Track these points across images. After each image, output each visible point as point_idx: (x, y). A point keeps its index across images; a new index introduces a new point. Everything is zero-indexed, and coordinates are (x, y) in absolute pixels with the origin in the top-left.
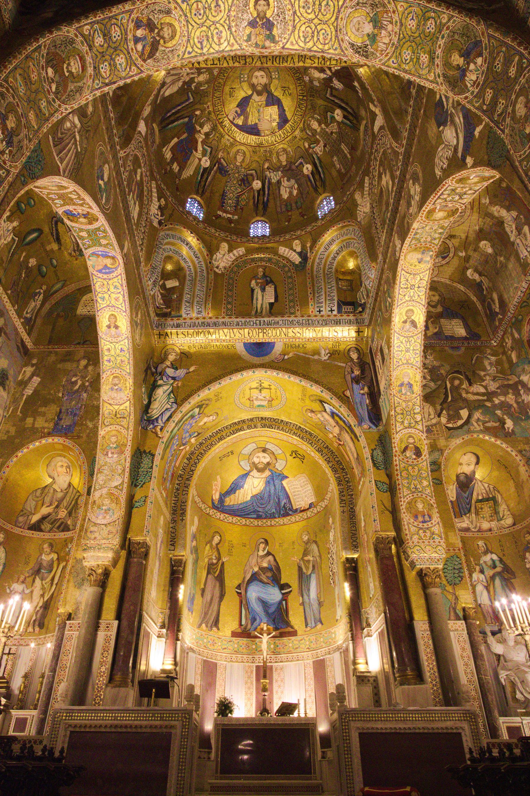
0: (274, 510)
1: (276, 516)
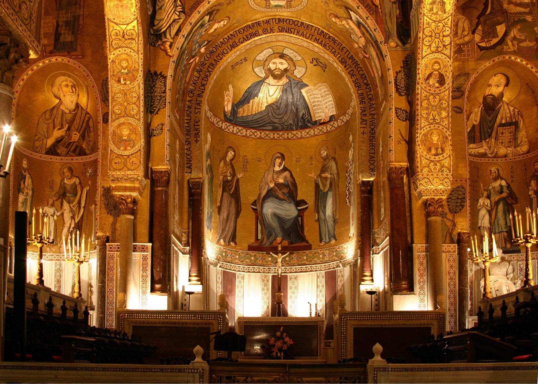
0: (291, 122)
1: (294, 128)
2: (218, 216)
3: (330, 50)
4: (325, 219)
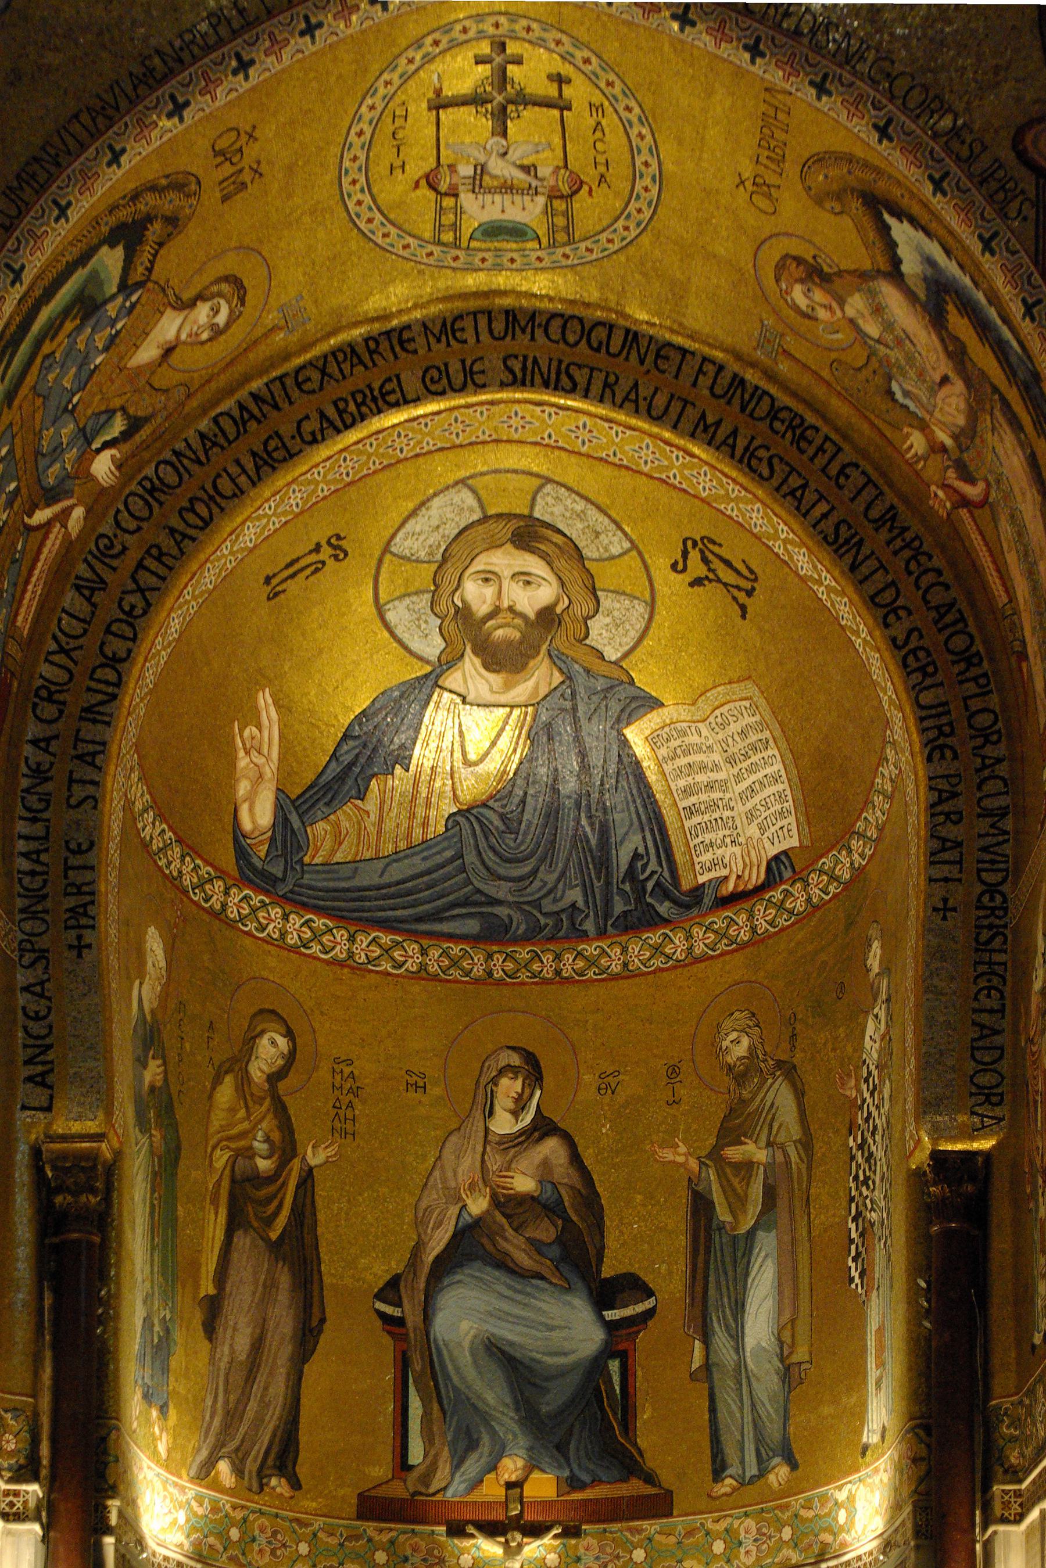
2: (206, 1345)
3: (775, 482)
4: (741, 1364)
